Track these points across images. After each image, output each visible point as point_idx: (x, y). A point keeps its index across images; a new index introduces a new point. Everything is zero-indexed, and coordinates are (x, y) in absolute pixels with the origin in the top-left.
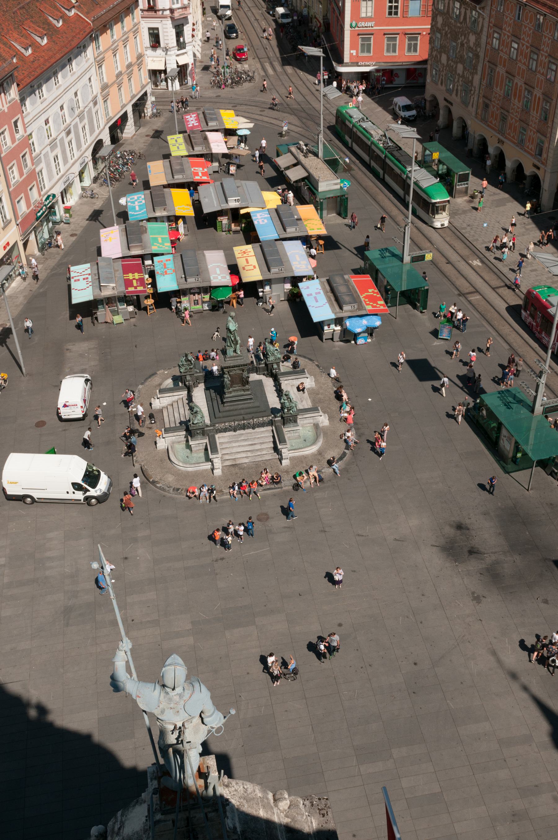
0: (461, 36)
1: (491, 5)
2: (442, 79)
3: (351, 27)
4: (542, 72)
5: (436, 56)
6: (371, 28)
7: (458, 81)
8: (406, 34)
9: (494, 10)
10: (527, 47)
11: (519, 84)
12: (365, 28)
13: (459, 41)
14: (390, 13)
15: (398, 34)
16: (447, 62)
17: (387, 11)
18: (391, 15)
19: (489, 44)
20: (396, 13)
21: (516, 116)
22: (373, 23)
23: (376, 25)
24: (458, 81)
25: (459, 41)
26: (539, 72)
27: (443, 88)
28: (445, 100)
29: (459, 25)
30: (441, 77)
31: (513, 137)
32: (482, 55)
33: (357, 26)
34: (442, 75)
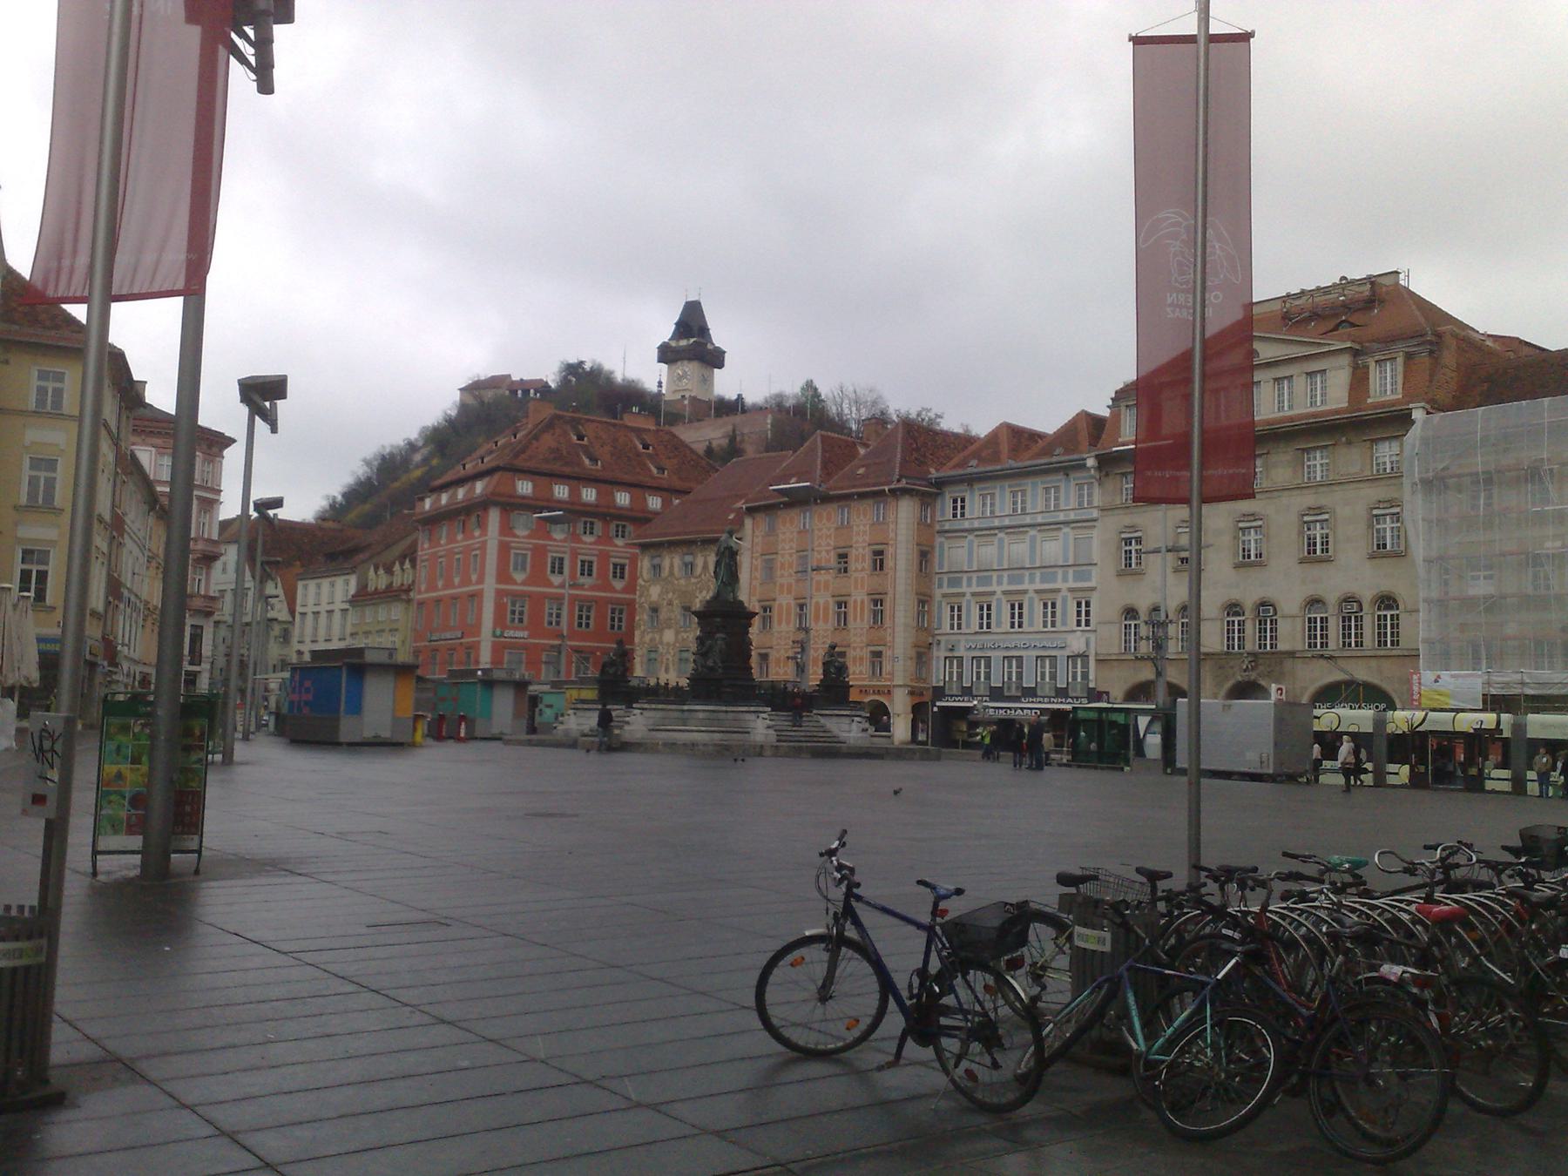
3: (494, 635)
10: (828, 552)
11: (821, 601)
22: (525, 634)
23: (530, 636)
33: (502, 636)
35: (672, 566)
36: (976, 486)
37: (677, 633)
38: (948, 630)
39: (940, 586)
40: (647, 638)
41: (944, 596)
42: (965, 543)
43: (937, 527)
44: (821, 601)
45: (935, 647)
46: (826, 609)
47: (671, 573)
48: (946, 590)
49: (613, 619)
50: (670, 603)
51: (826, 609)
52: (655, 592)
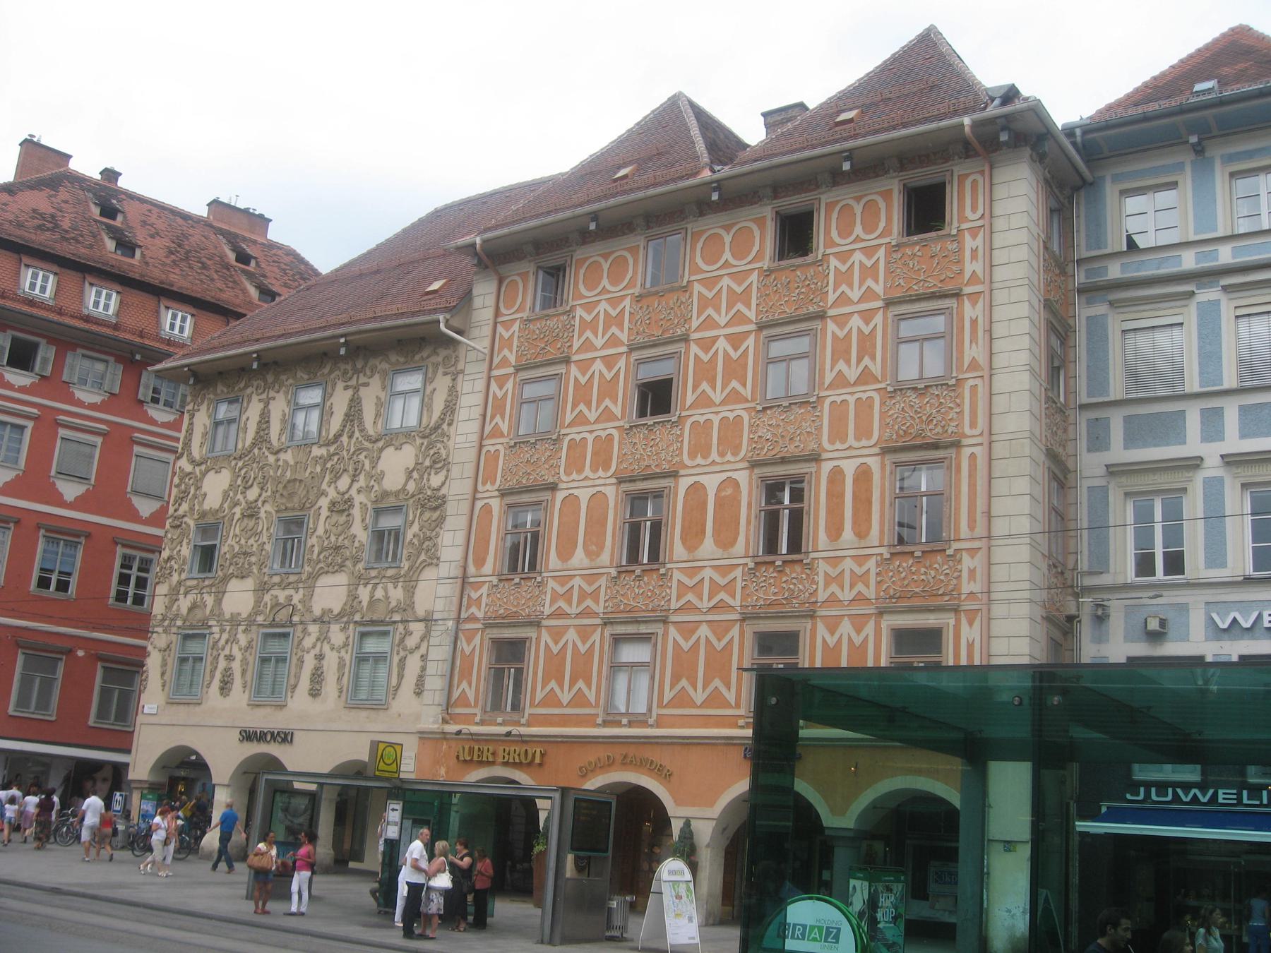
0: (336, 477)
1: (497, 313)
4: (852, 374)
9: (507, 324)
11: (711, 483)
13: (324, 503)
16: (258, 602)
19: (496, 433)
25: (324, 503)
26: (840, 381)
27: (239, 697)
28: (248, 736)
29: (317, 451)
30: (222, 664)
31: (715, 699)
32: (457, 487)
34: (230, 658)
35: (265, 419)
36: (1216, 152)
37: (262, 588)
38: (1130, 576)
39: (1098, 441)
40: (184, 604)
41: (1114, 471)
42: (1190, 314)
43: (1080, 277)
44: (711, 483)
45: (1086, 628)
46: (727, 504)
47: (262, 437)
48: (1119, 453)
49: (124, 579)
50: (251, 513)
51: (727, 504)
52: (215, 486)
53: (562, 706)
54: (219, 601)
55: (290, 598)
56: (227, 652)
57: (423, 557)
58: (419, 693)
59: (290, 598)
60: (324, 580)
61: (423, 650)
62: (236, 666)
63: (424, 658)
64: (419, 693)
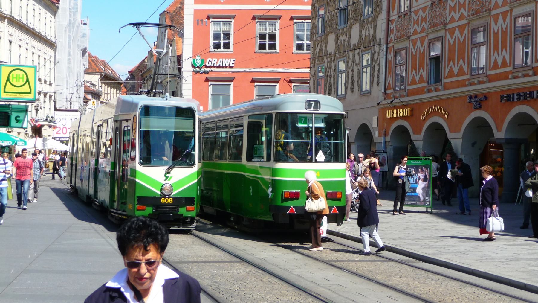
2: (330, 82)
5: (321, 49)
6: (228, 70)
7: (354, 61)
8: (291, 81)
12: (218, 70)
14: (262, 46)
15: (277, 81)
17: (257, 42)
18: (265, 48)
20: (272, 46)
21: (461, 17)
23: (237, 64)
24: (354, 61)
30: (329, 79)
34: (330, 76)
53: (416, 84)
54: (326, 47)
55: (344, 40)
56: (329, 74)
57: (378, 9)
58: (378, 84)
59: (344, 40)
60: (353, 27)
61: (378, 62)
62: (332, 79)
63: (379, 65)
64: (378, 84)
